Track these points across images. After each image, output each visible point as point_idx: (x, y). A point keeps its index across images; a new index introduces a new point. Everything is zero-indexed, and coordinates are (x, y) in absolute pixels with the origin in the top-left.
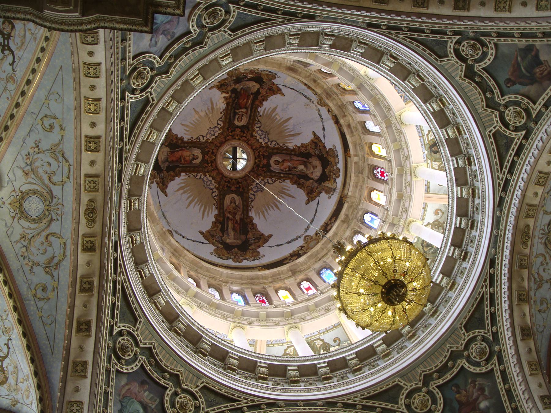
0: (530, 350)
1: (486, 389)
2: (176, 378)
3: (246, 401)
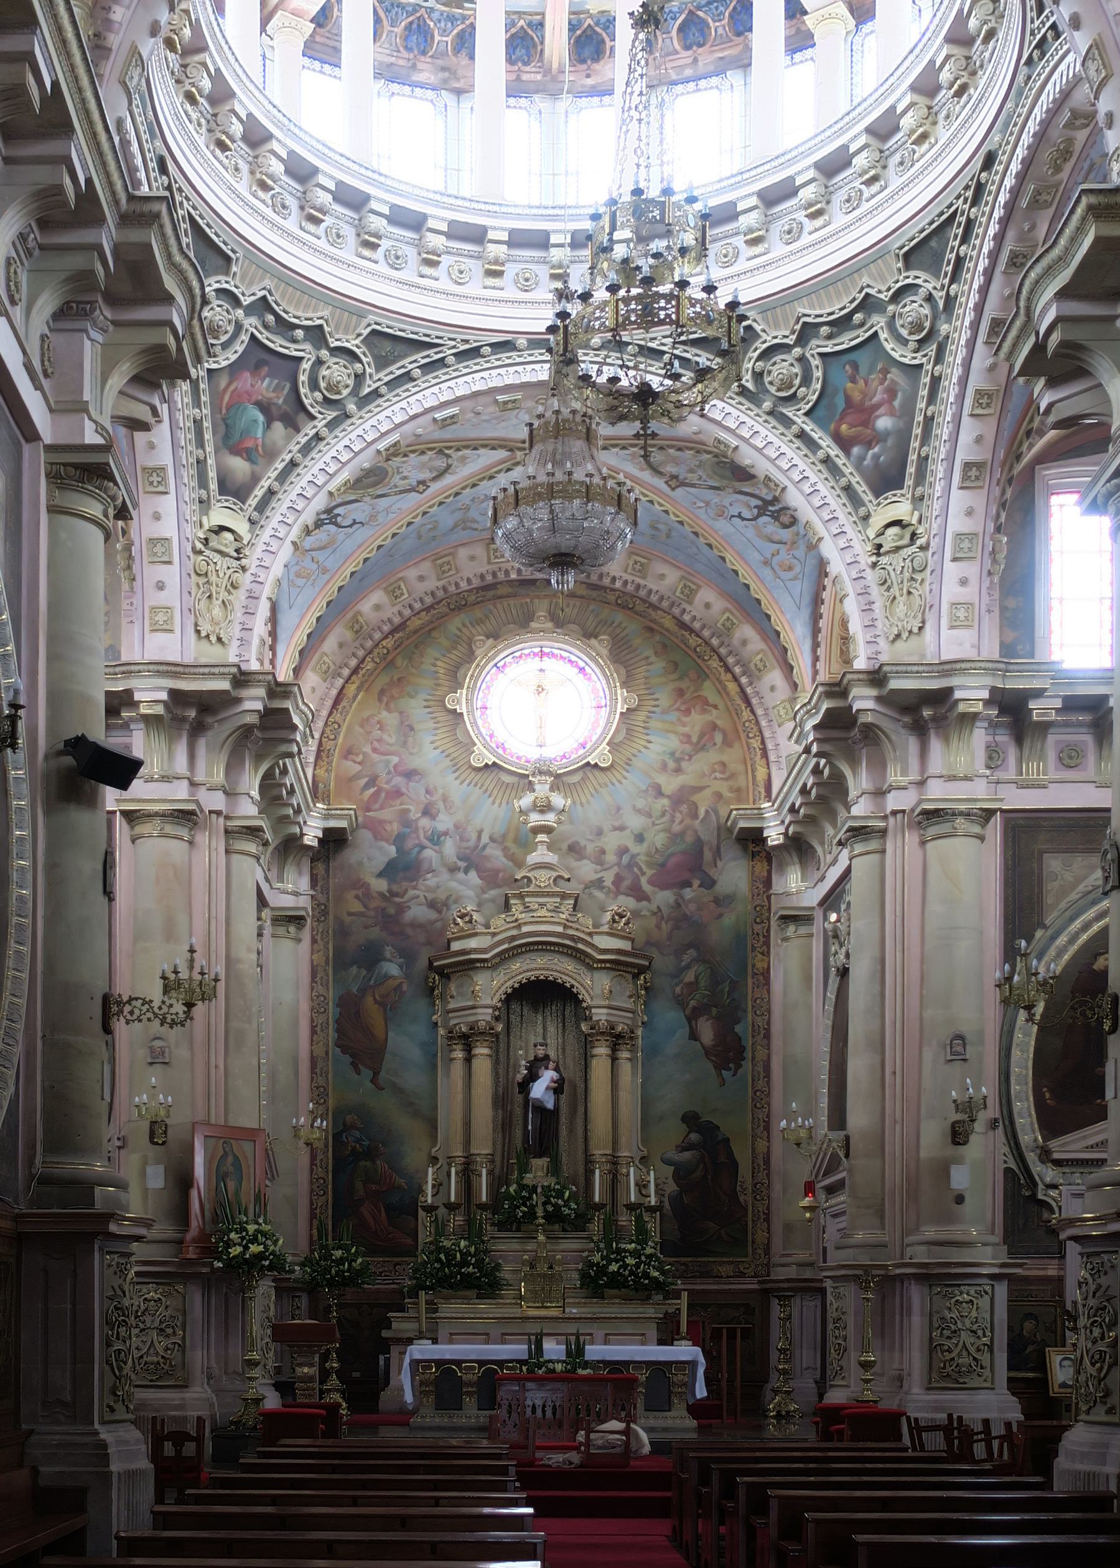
0: (992, 368)
1: (899, 395)
2: (316, 335)
3: (453, 343)
